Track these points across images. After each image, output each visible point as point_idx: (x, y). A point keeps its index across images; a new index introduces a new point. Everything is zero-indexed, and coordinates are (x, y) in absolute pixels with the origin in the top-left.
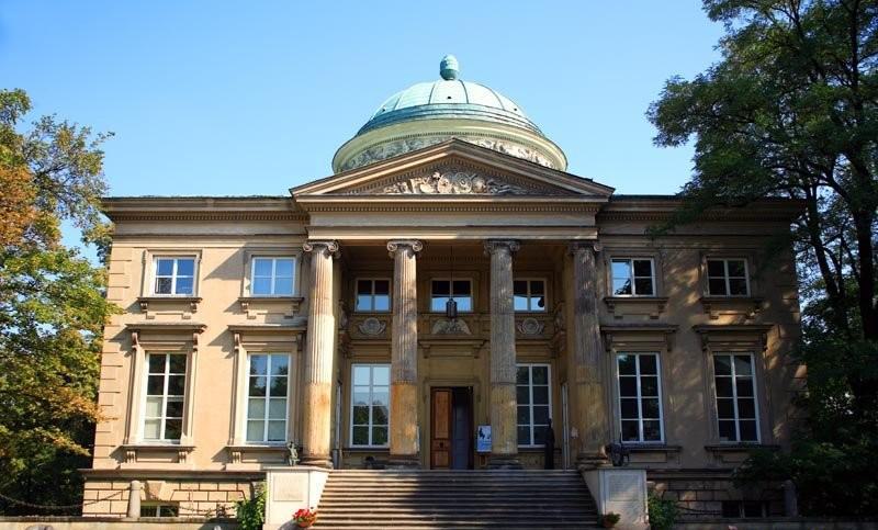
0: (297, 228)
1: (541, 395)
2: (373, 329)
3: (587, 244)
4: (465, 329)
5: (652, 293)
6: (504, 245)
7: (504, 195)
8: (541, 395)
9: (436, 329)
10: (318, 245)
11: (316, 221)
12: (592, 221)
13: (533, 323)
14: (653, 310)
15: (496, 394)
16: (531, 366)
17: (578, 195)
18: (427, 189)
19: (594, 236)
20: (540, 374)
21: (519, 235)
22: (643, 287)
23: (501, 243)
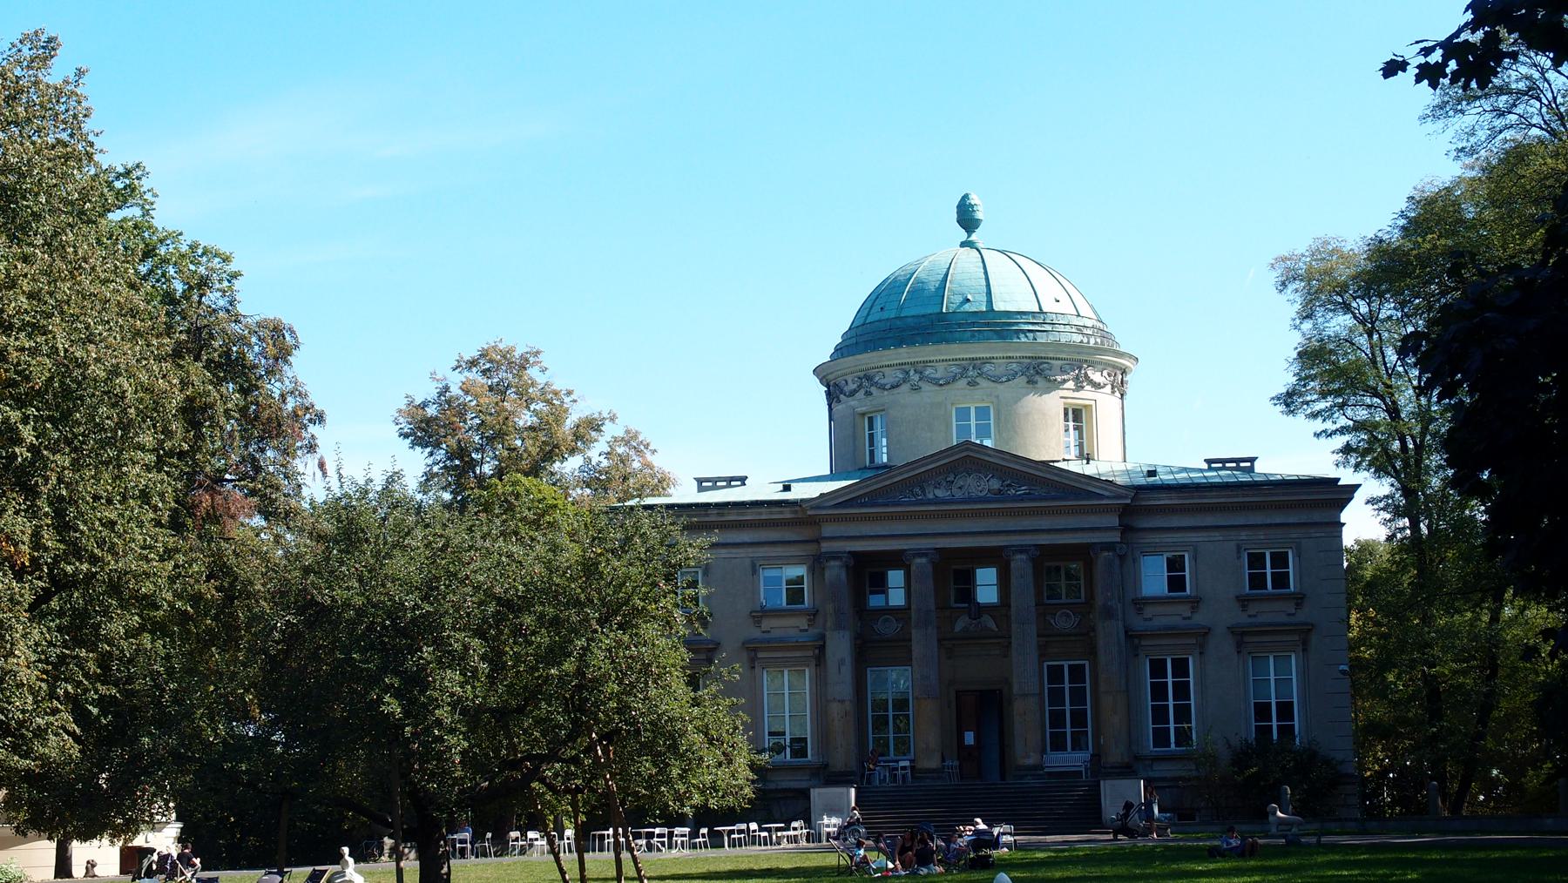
0: (806, 533)
1: (1077, 695)
2: (889, 628)
3: (1109, 546)
4: (992, 625)
5: (1184, 590)
6: (1021, 552)
7: (1021, 499)
8: (1077, 695)
9: (958, 627)
10: (834, 556)
11: (828, 530)
12: (1115, 521)
13: (1068, 615)
14: (1185, 610)
15: (1018, 706)
16: (1066, 664)
17: (1101, 497)
18: (940, 493)
19: (1115, 537)
20: (1077, 673)
21: (1044, 539)
22: (1176, 583)
23: (1022, 549)
